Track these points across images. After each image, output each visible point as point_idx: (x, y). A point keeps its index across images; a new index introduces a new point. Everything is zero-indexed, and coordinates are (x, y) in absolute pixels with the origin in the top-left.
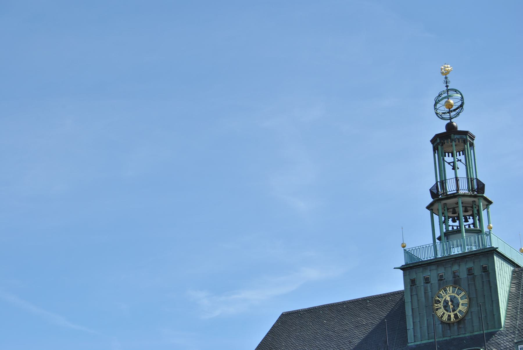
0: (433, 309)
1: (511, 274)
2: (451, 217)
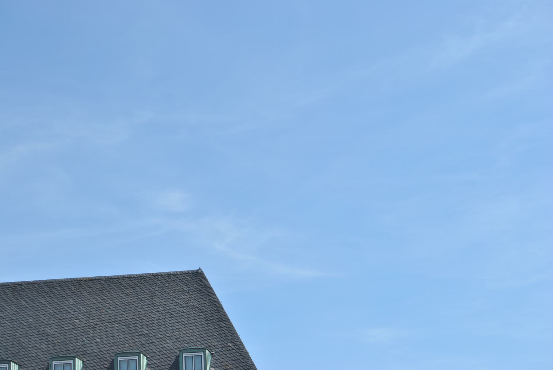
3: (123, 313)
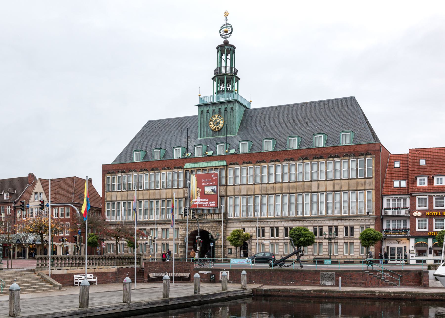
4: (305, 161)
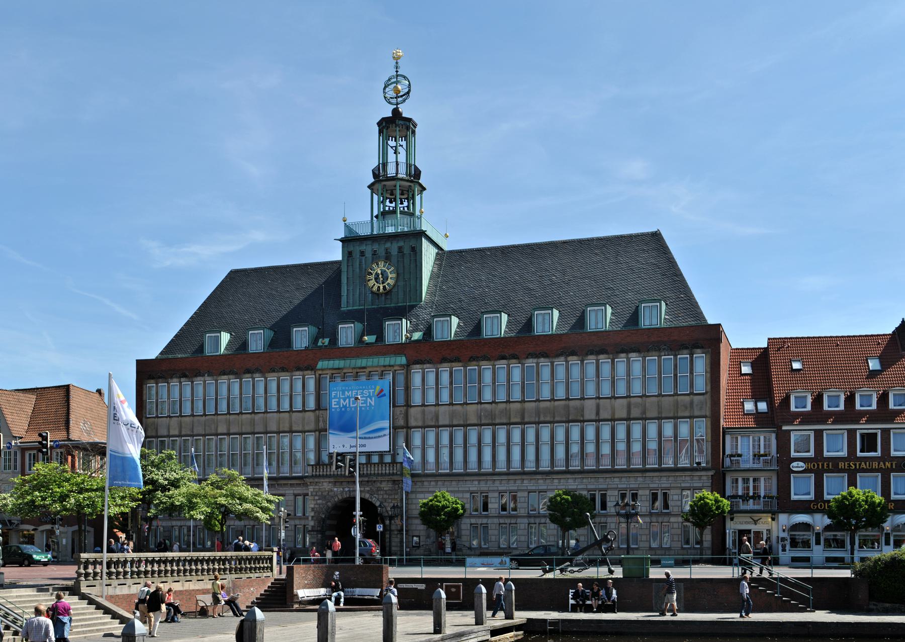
0: (366, 279)
1: (435, 256)
2: (389, 198)
3: (592, 270)
4: (570, 358)
